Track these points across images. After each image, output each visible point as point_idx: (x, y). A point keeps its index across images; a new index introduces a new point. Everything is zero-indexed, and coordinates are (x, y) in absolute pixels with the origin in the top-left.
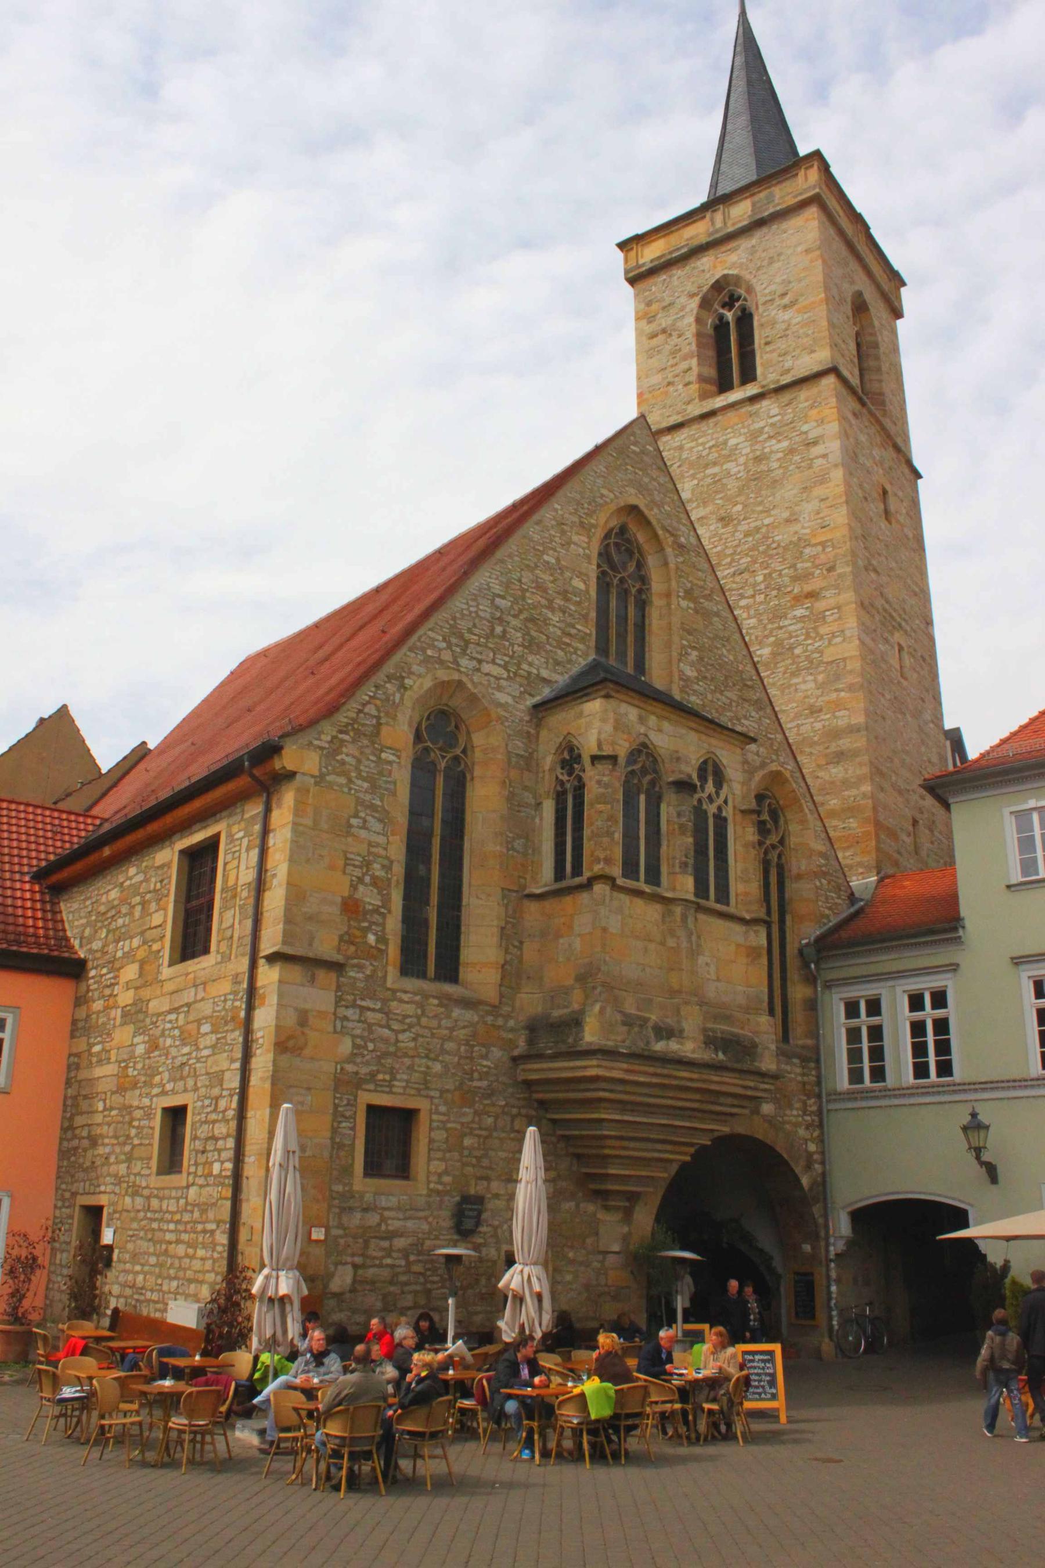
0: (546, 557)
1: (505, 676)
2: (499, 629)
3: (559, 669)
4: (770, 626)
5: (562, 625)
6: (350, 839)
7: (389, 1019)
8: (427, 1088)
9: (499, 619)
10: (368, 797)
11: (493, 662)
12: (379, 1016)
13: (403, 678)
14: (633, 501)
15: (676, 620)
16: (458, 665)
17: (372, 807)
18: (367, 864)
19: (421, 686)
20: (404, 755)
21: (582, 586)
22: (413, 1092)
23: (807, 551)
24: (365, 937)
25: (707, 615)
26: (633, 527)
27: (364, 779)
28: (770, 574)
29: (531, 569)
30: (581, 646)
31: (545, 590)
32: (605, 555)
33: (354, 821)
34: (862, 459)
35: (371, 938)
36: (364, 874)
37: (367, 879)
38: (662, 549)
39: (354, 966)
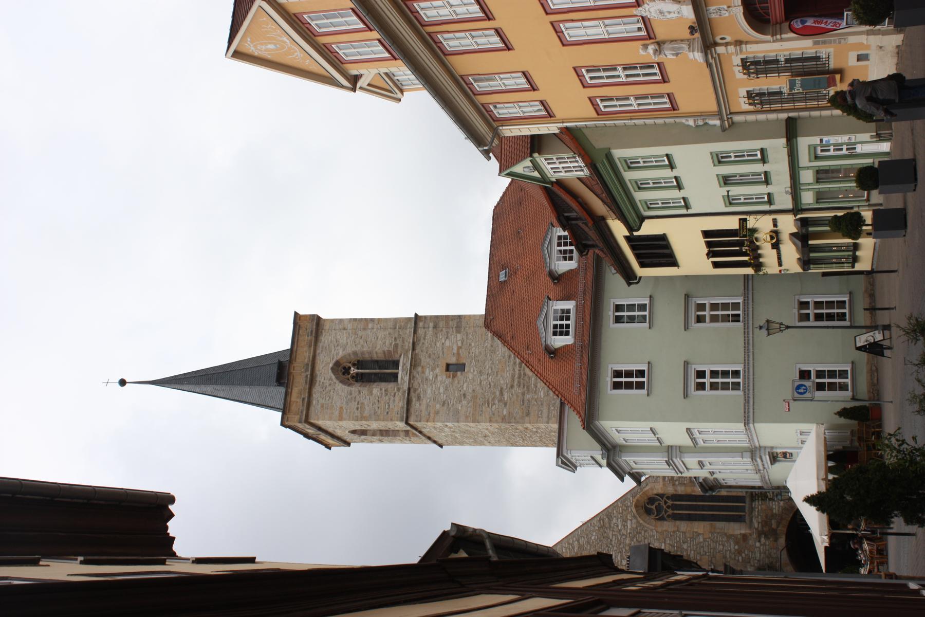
34: (443, 397)
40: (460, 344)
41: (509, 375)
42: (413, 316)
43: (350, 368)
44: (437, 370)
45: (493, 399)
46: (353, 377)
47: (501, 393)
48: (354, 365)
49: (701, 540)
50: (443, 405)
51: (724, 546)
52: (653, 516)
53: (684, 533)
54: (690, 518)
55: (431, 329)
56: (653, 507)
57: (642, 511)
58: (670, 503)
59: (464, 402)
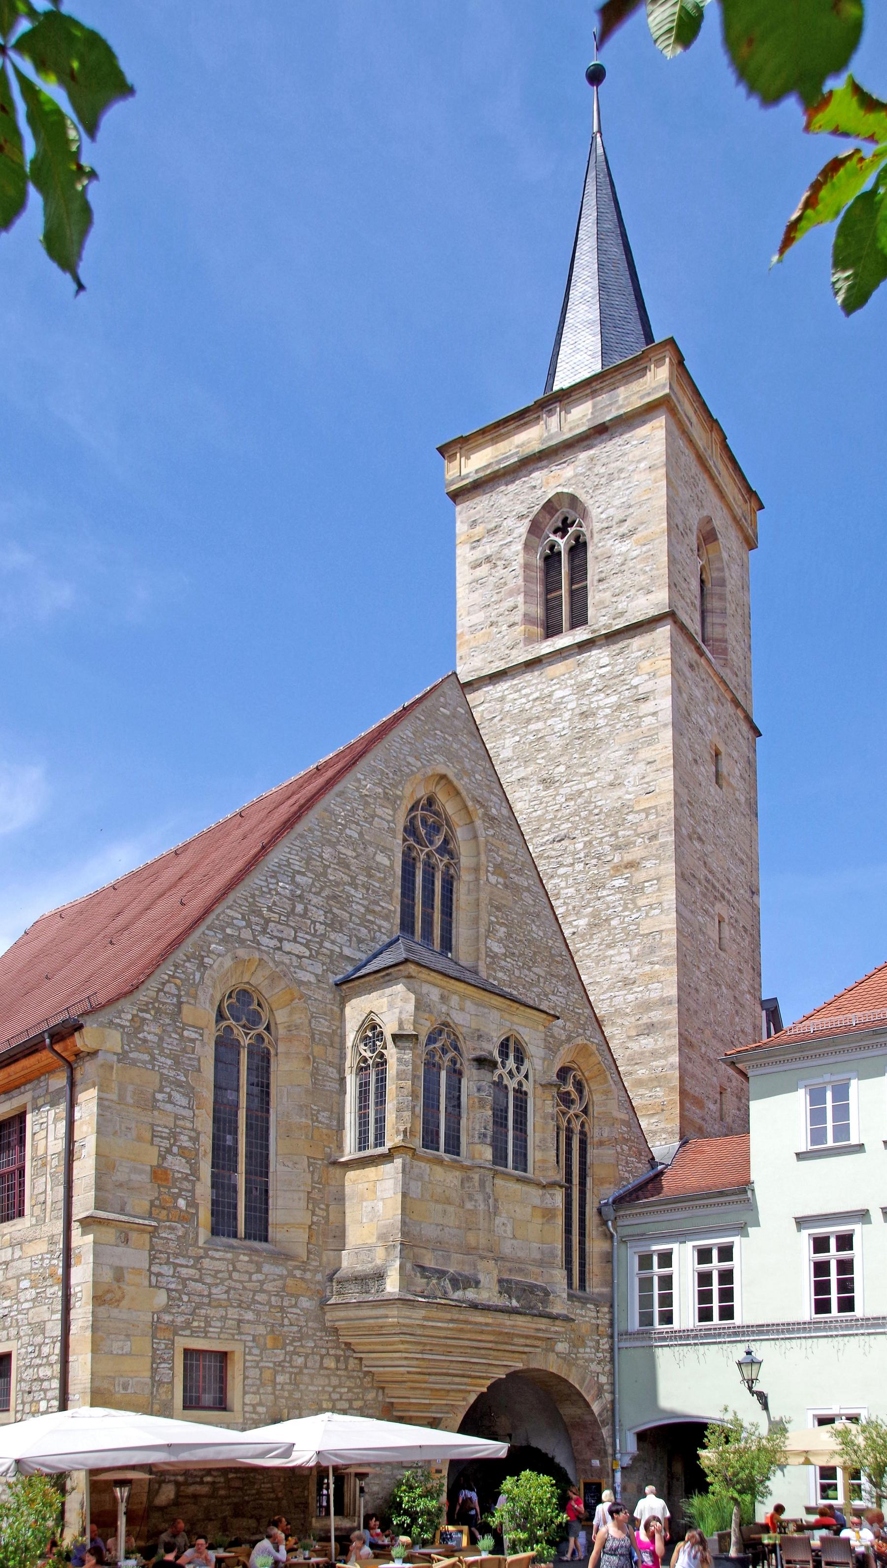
0: (348, 831)
1: (307, 954)
2: (299, 908)
3: (363, 947)
4: (588, 896)
5: (366, 903)
6: (156, 1113)
7: (201, 1275)
8: (240, 1333)
9: (300, 897)
10: (172, 1073)
11: (295, 940)
12: (192, 1271)
13: (203, 957)
14: (442, 770)
15: (484, 896)
16: (259, 944)
17: (179, 1084)
18: (174, 1136)
19: (221, 965)
20: (206, 1032)
21: (387, 862)
22: (226, 1336)
23: (630, 817)
24: (176, 1202)
25: (516, 889)
27: (168, 1057)
28: (590, 842)
29: (333, 845)
30: (385, 924)
31: (348, 866)
32: (410, 830)
33: (159, 1096)
35: (182, 1203)
36: (172, 1146)
37: (175, 1150)
38: (472, 822)
39: (166, 1227)
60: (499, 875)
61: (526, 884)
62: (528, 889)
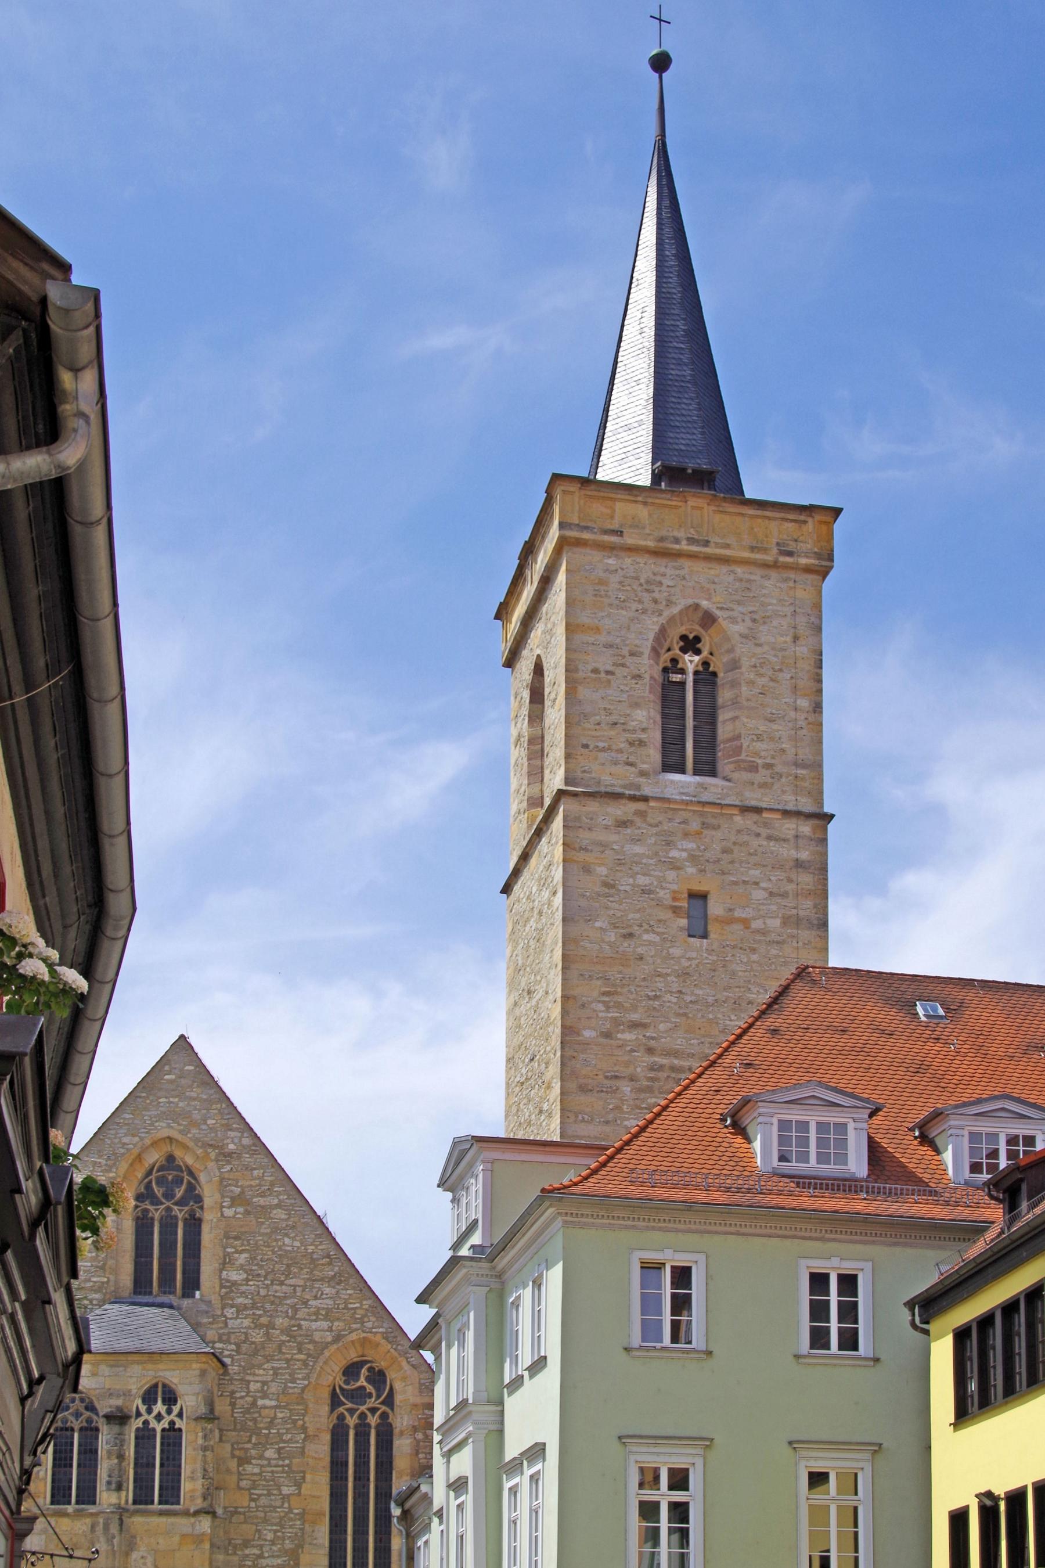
14: (165, 1133)
26: (178, 1153)
34: (625, 884)
40: (756, 924)
41: (679, 1042)
42: (827, 809)
43: (698, 652)
44: (691, 870)
45: (619, 1005)
46: (674, 661)
47: (635, 1025)
48: (706, 664)
49: (285, 1490)
50: (606, 884)
51: (273, 1543)
52: (340, 1380)
53: (302, 1452)
54: (337, 1468)
55: (793, 854)
56: (362, 1382)
57: (353, 1356)
58: (373, 1420)
59: (612, 936)
60: (240, 1205)
61: (276, 1201)
62: (278, 1206)
